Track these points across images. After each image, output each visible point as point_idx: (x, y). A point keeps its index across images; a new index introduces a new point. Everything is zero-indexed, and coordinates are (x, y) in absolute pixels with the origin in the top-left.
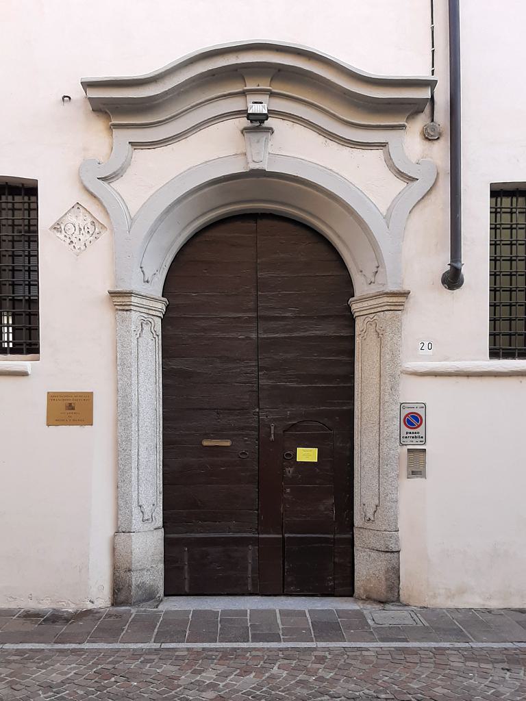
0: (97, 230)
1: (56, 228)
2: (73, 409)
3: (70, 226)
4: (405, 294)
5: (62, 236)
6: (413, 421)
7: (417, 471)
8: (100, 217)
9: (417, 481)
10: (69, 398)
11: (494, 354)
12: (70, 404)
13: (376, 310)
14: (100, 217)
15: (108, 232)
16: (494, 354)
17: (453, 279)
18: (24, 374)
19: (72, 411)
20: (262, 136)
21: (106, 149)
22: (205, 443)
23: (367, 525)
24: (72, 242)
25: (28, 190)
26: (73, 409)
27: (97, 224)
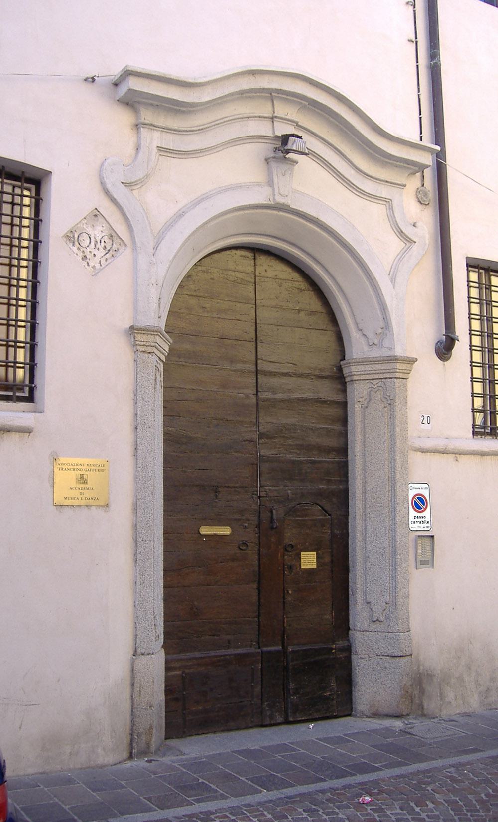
0: (115, 247)
1: (72, 237)
2: (85, 482)
3: (85, 236)
4: (412, 361)
5: (75, 249)
6: (420, 504)
7: (427, 562)
8: (121, 229)
9: (425, 571)
10: (80, 467)
11: (477, 432)
12: (82, 475)
13: (381, 376)
14: (121, 229)
15: (129, 250)
16: (477, 432)
17: (445, 349)
18: (28, 431)
19: (83, 486)
20: (285, 167)
21: (130, 150)
22: (205, 530)
23: (373, 626)
24: (85, 256)
25: (34, 180)
26: (85, 482)
27: (115, 239)
